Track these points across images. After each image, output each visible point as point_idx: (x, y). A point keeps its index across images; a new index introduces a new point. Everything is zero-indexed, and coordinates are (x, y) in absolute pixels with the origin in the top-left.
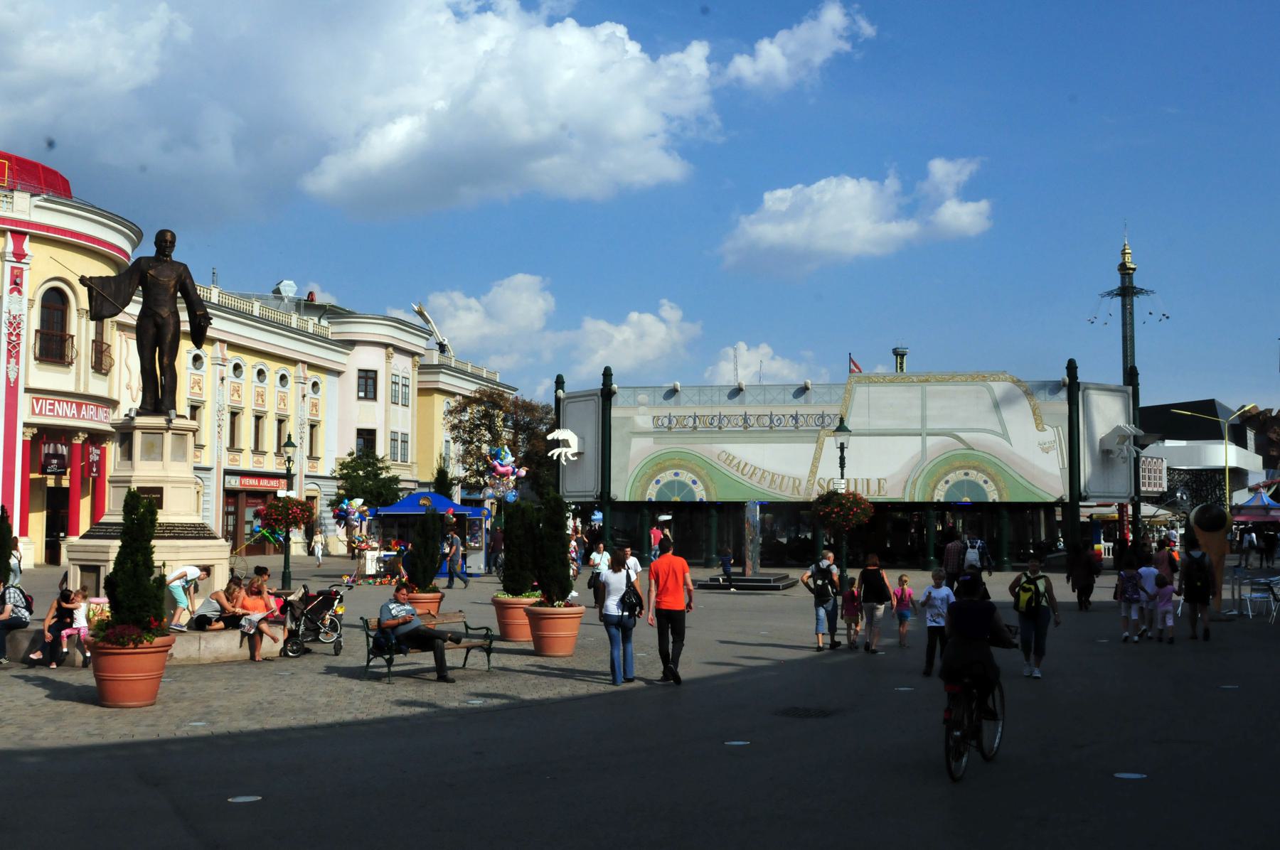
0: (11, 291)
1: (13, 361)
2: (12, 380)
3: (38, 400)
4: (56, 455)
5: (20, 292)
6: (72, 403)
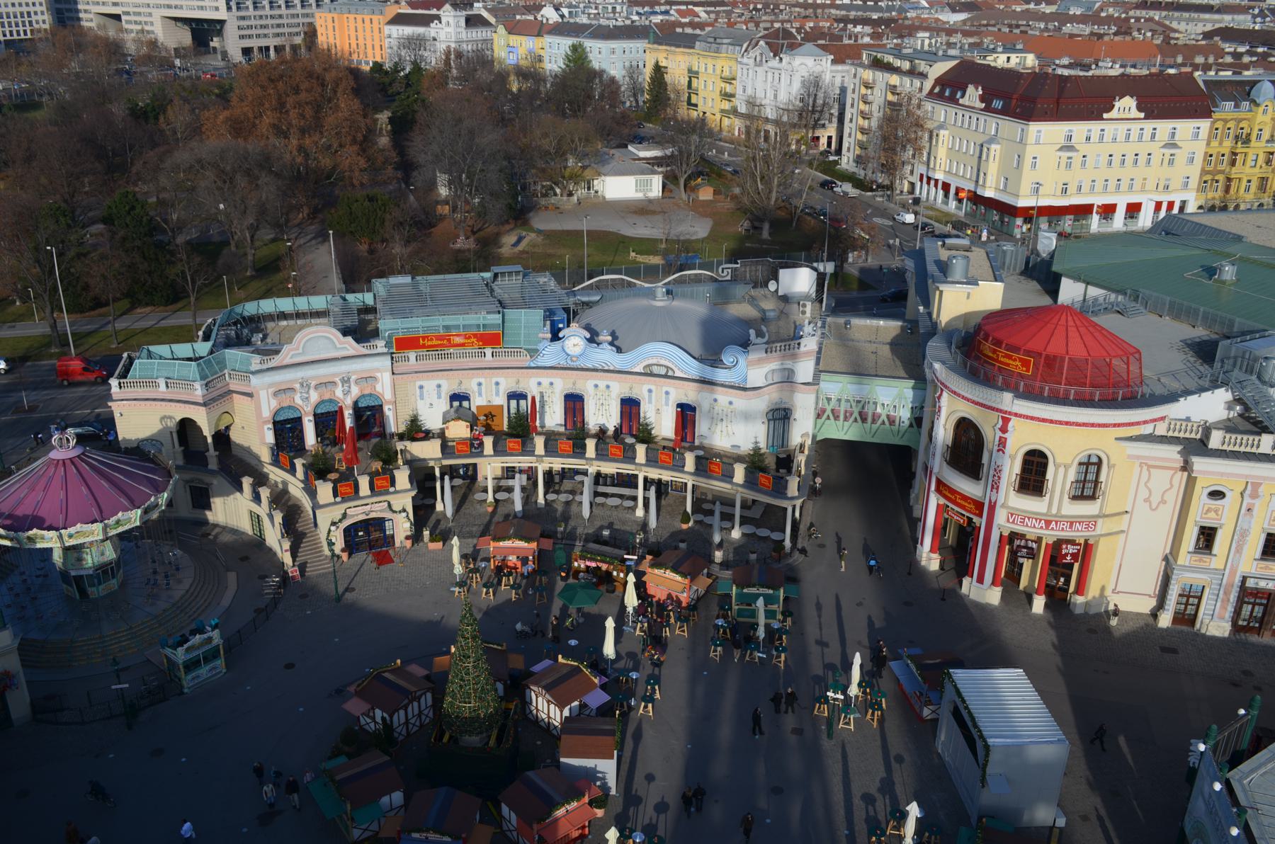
0: (998, 451)
3: (1012, 515)
4: (1026, 547)
6: (1041, 520)
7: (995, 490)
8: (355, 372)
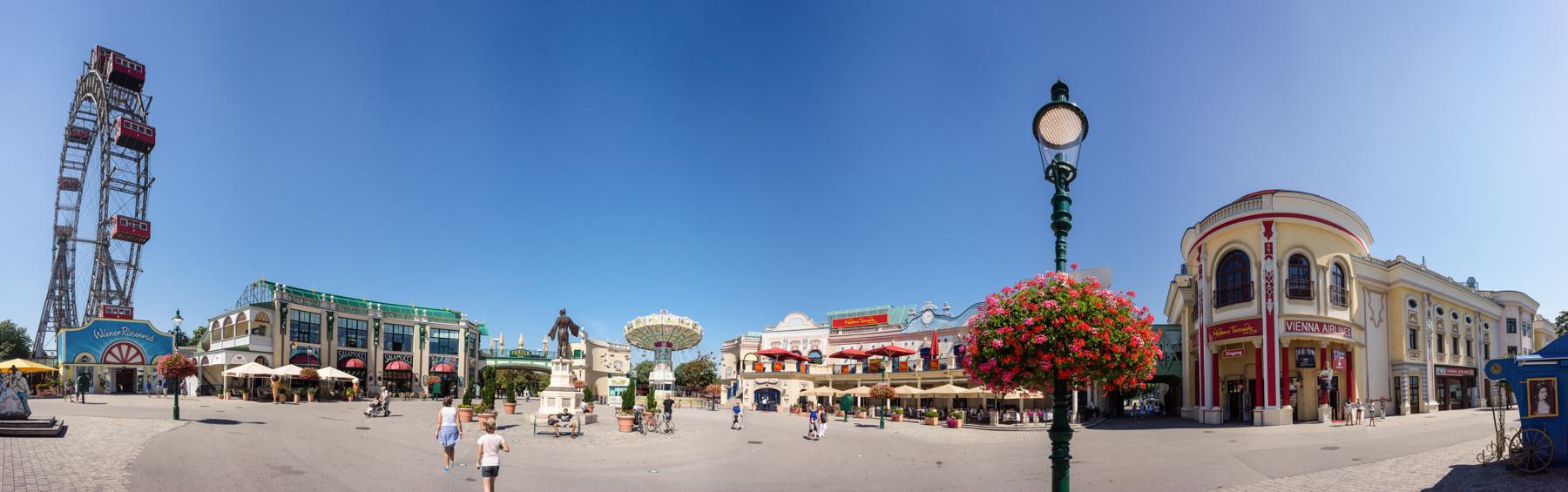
0: (1266, 258)
1: (1270, 300)
2: (1270, 311)
4: (1306, 356)
5: (1272, 258)
7: (1270, 300)
8: (811, 337)
